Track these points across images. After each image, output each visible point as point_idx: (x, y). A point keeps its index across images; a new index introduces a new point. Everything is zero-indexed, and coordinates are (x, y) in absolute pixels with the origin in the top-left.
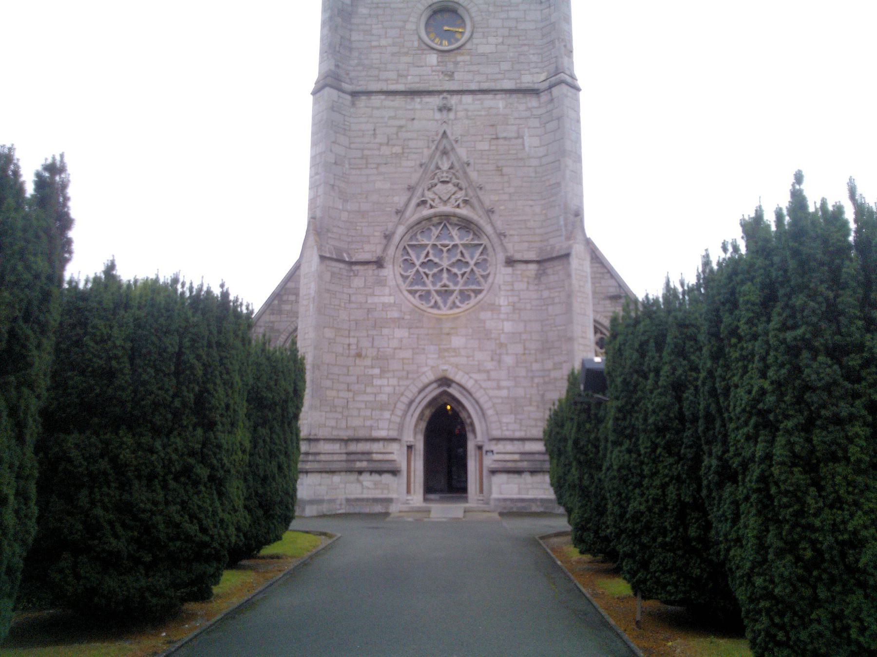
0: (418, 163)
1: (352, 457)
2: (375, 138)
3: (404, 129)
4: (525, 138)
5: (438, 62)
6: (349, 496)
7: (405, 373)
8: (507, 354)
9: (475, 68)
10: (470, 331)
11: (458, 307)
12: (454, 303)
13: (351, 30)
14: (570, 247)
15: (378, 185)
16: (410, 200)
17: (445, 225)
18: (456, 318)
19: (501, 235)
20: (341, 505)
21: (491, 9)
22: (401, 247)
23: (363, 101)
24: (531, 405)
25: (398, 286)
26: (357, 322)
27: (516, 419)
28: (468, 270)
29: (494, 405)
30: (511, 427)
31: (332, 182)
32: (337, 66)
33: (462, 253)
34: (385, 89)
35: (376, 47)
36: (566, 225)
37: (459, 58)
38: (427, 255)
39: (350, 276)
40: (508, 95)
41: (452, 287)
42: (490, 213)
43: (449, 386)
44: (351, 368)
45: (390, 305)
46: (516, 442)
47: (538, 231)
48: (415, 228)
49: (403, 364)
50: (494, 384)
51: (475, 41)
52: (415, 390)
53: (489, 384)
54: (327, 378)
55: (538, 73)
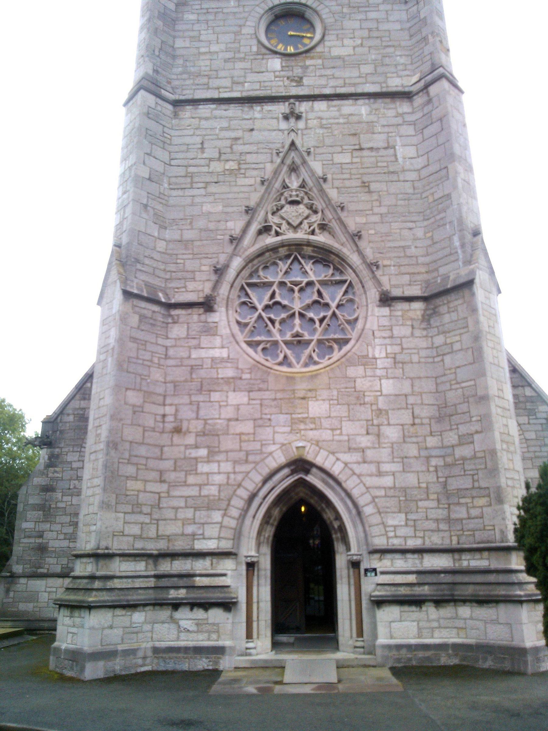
0: (259, 180)
1: (164, 582)
2: (203, 152)
3: (240, 142)
4: (397, 147)
5: (282, 67)
6: (157, 644)
7: (242, 455)
8: (389, 424)
9: (329, 72)
10: (335, 393)
11: (316, 363)
12: (310, 357)
13: (174, 37)
14: (473, 272)
15: (207, 208)
16: (248, 224)
17: (296, 258)
18: (314, 376)
19: (373, 266)
20: (145, 658)
21: (345, 10)
22: (237, 285)
23: (188, 112)
24: (428, 499)
25: (233, 336)
26: (175, 384)
27: (407, 519)
28: (330, 313)
29: (374, 498)
30: (401, 532)
31: (145, 202)
32: (156, 71)
33: (320, 293)
34: (216, 96)
35: (205, 53)
36: (463, 246)
37: (308, 62)
38: (273, 296)
39: (168, 323)
40: (372, 100)
41: (307, 337)
42: (356, 239)
43: (307, 472)
44: (166, 449)
45: (222, 360)
46: (409, 556)
47: (421, 260)
48: (255, 262)
49: (241, 441)
50: (373, 468)
51: (327, 44)
52: (258, 479)
54: (129, 462)
55: (408, 76)
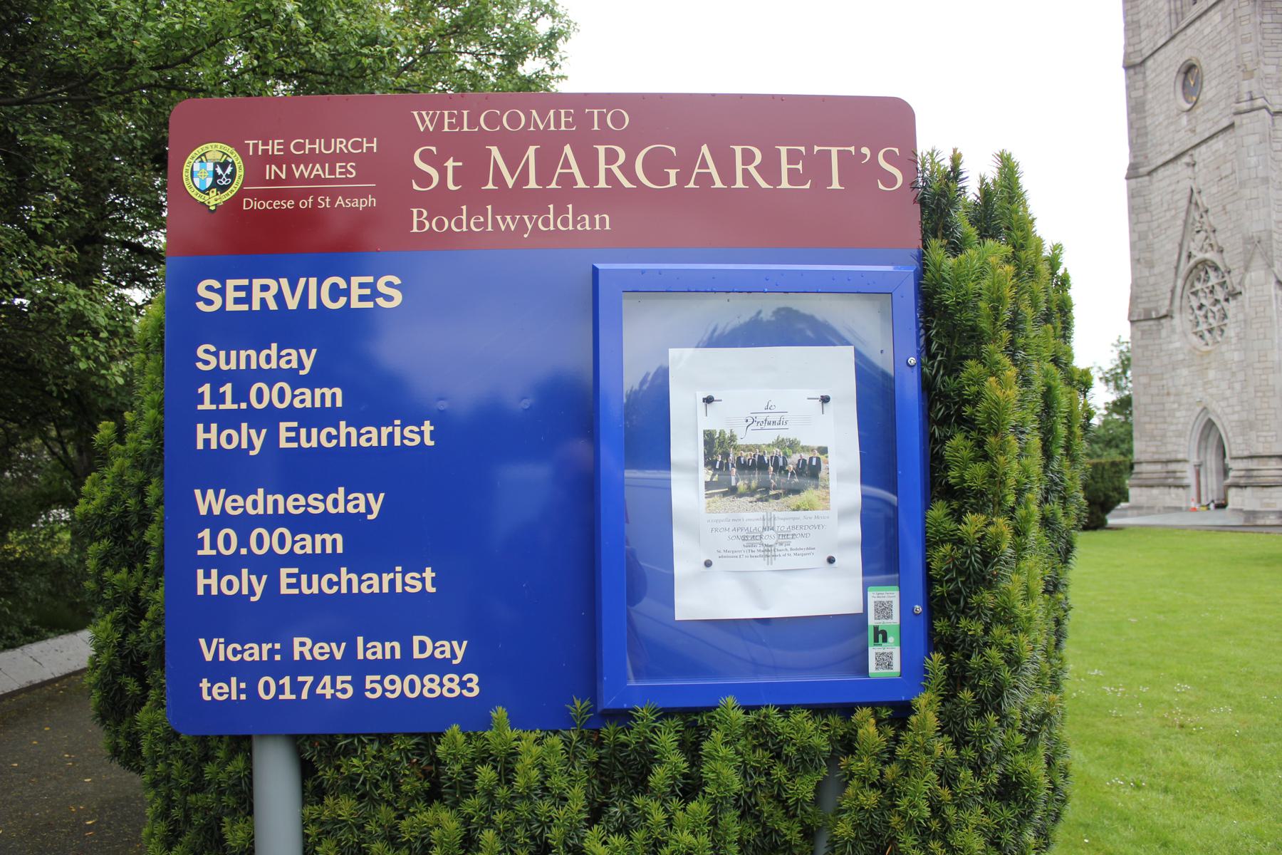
31: (1137, 257)
48: (1190, 278)
53: (1228, 410)
